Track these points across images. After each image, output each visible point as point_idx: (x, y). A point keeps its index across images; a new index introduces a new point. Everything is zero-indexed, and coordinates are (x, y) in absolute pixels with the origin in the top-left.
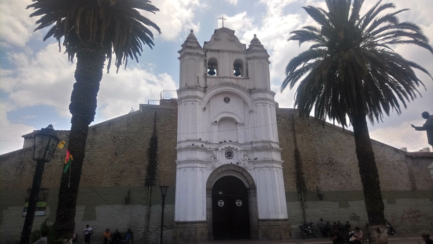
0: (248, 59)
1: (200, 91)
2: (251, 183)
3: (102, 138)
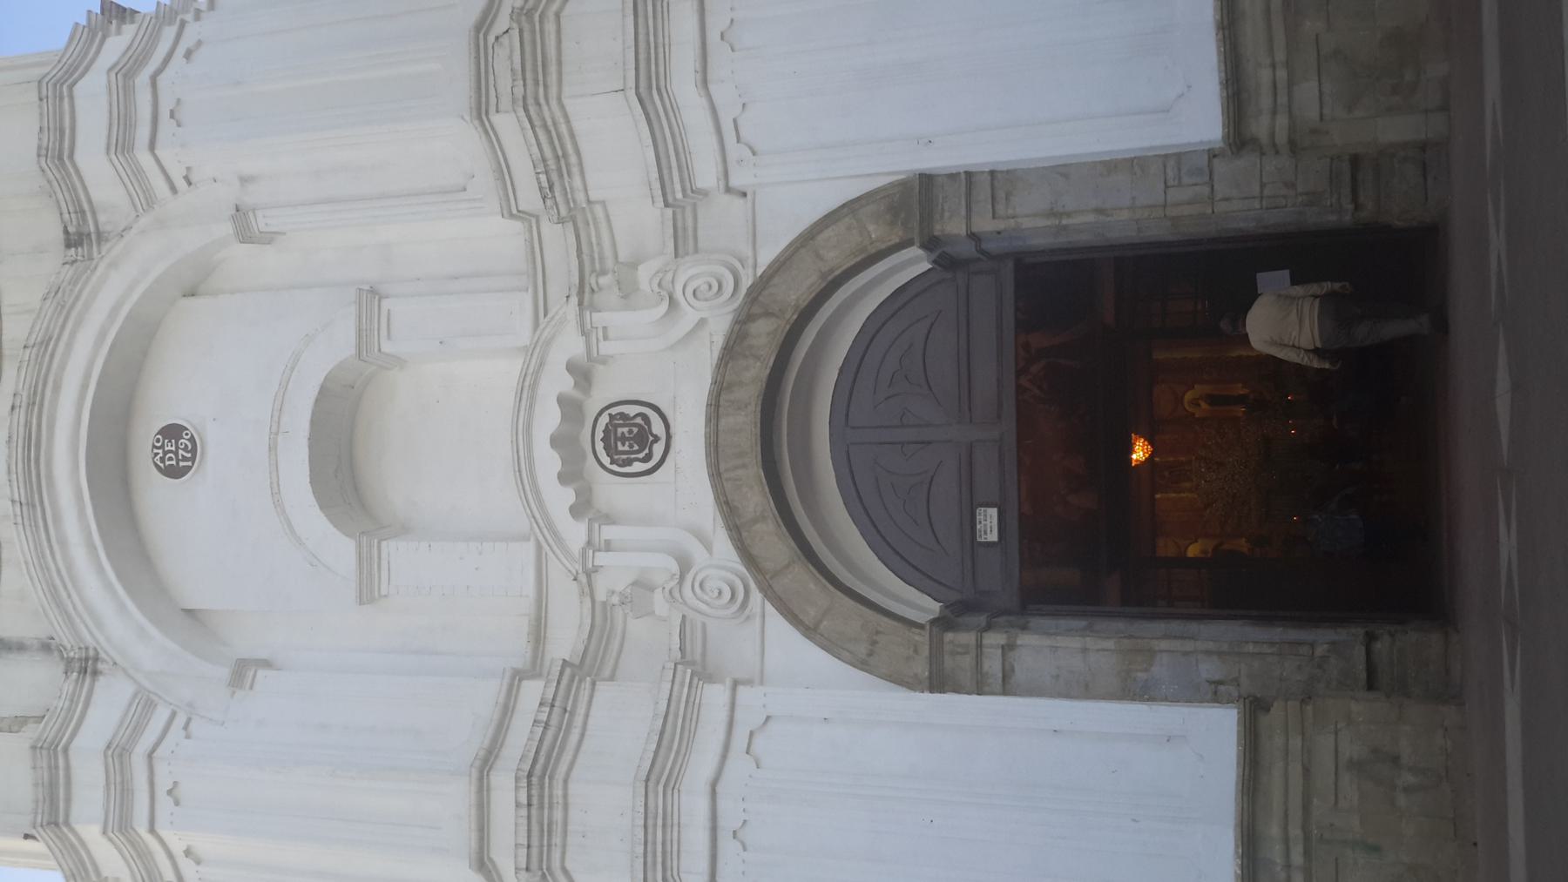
1: (74, 715)
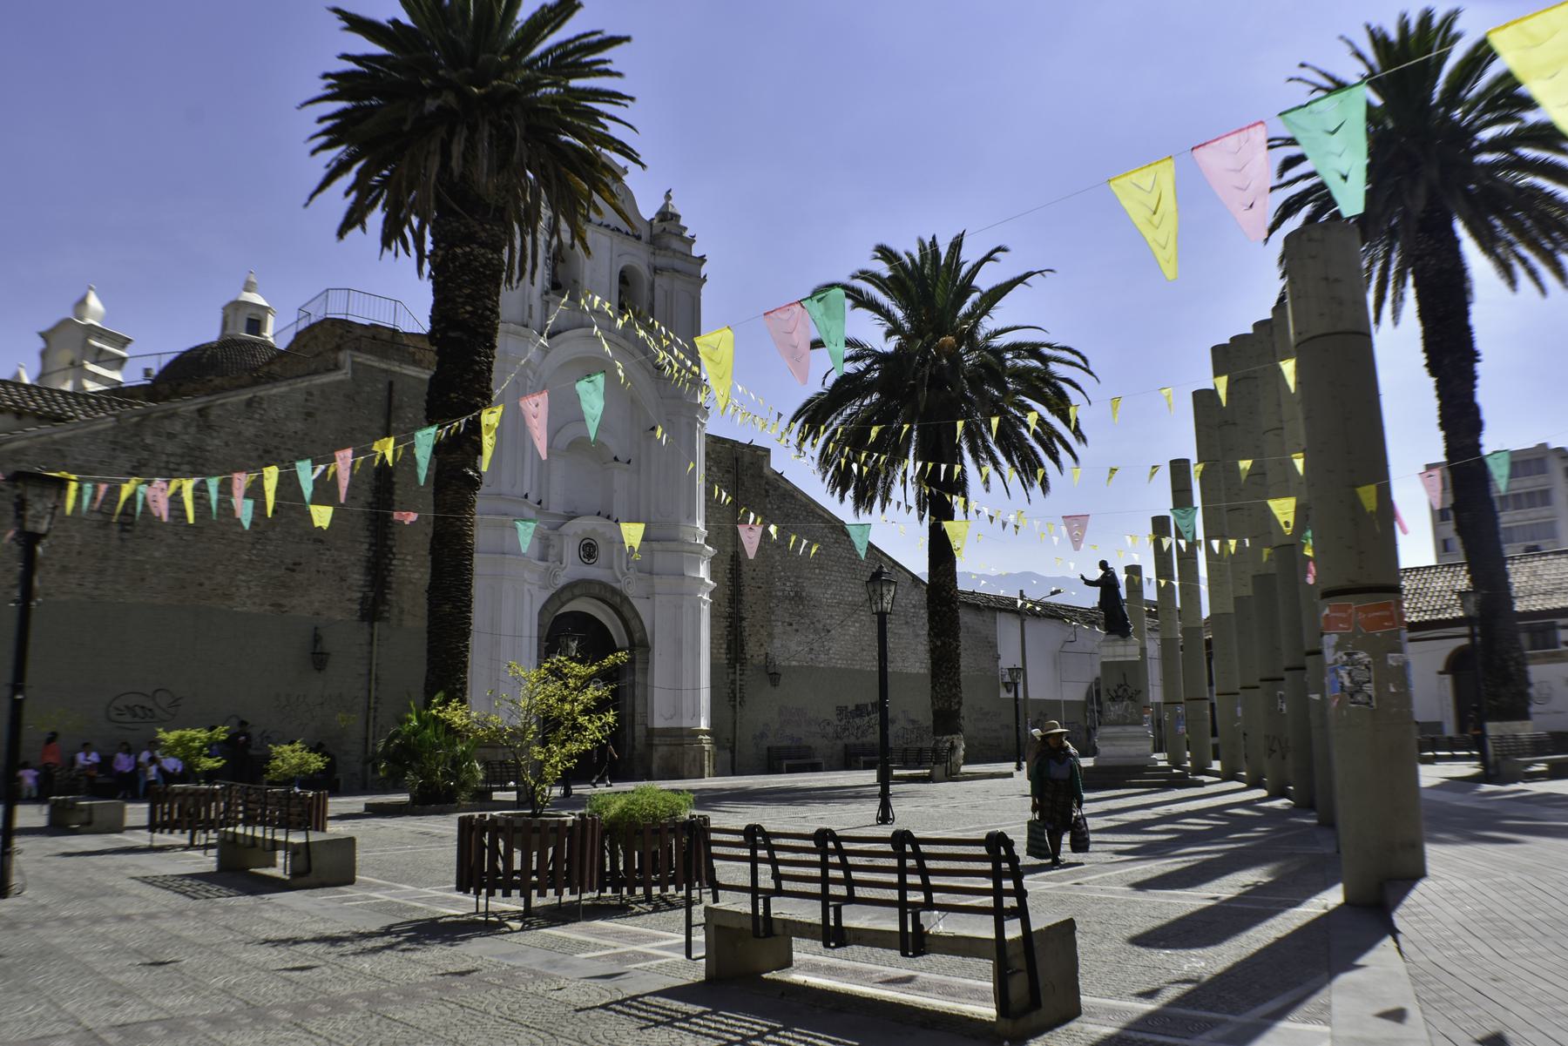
0: (656, 270)
2: (637, 636)
3: (227, 444)
